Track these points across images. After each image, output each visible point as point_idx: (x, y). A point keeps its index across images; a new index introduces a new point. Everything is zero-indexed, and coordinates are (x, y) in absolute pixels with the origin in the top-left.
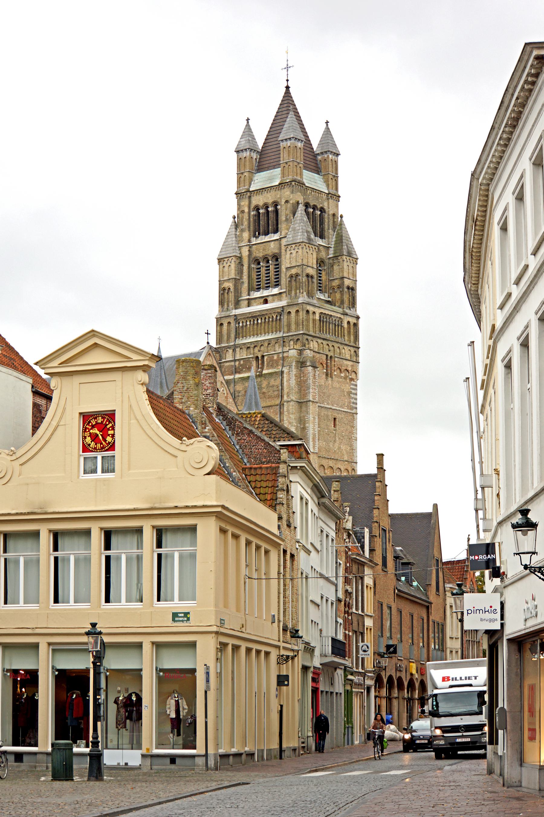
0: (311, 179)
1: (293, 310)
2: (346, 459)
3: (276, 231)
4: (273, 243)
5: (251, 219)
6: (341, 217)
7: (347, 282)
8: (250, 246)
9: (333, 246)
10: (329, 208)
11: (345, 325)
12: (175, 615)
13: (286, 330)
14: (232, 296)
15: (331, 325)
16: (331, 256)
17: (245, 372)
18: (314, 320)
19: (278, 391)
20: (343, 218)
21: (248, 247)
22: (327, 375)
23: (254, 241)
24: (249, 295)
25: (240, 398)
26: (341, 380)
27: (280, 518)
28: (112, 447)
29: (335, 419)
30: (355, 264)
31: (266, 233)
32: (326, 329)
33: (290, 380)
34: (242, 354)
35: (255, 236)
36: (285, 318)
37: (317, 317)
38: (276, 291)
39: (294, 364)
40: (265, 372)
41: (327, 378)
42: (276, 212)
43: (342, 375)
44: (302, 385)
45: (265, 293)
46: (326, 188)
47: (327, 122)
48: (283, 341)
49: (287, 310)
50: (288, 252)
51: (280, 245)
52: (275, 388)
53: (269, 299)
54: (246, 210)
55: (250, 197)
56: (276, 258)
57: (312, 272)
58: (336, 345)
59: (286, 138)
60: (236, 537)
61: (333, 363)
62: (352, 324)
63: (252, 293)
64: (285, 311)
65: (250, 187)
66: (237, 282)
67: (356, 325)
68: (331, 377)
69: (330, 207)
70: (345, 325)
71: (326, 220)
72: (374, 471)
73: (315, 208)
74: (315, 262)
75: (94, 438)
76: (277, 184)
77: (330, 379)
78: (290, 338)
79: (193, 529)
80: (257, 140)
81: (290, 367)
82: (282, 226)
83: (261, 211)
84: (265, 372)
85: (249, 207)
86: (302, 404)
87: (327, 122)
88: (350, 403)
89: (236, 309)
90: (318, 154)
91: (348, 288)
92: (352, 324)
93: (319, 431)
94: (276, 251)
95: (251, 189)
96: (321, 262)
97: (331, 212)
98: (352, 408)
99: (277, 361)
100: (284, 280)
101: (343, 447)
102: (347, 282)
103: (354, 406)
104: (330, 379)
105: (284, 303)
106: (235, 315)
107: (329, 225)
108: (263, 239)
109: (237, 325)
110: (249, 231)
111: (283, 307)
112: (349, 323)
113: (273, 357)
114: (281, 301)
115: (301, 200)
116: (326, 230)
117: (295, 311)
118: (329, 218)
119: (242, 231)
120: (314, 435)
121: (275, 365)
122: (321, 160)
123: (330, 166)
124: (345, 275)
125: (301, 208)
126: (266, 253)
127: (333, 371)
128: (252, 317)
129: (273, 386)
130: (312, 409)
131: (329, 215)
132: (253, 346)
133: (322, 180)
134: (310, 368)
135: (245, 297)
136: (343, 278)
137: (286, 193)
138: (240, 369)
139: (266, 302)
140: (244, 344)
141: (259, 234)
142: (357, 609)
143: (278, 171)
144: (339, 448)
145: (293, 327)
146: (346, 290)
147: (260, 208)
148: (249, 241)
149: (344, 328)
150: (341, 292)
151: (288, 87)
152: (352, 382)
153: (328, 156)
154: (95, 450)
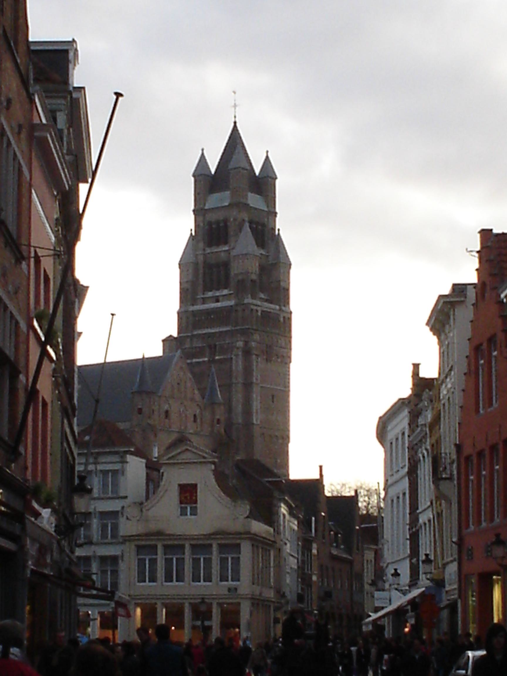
0: (254, 200)
3: (226, 243)
6: (279, 230)
8: (204, 255)
11: (282, 319)
12: (229, 590)
22: (267, 360)
23: (208, 250)
27: (274, 530)
28: (196, 502)
31: (218, 245)
33: (238, 365)
34: (198, 344)
37: (259, 314)
38: (225, 292)
39: (240, 353)
42: (226, 226)
43: (279, 360)
44: (248, 371)
45: (218, 294)
46: (266, 207)
53: (221, 299)
56: (226, 265)
57: (254, 277)
60: (257, 547)
63: (206, 292)
65: (205, 205)
67: (290, 319)
70: (282, 319)
72: (317, 477)
73: (257, 223)
74: (257, 269)
75: (186, 497)
76: (227, 204)
79: (238, 546)
81: (237, 355)
83: (214, 226)
84: (217, 358)
85: (203, 222)
86: (248, 385)
89: (193, 305)
91: (284, 289)
93: (261, 407)
96: (262, 268)
104: (269, 364)
105: (232, 303)
106: (193, 311)
108: (215, 249)
110: (204, 243)
111: (231, 306)
112: (284, 317)
114: (230, 300)
115: (246, 219)
120: (257, 410)
122: (264, 183)
125: (247, 224)
134: (254, 356)
137: (234, 213)
139: (218, 301)
142: (308, 570)
143: (228, 193)
148: (204, 250)
151: (235, 123)
154: (186, 503)
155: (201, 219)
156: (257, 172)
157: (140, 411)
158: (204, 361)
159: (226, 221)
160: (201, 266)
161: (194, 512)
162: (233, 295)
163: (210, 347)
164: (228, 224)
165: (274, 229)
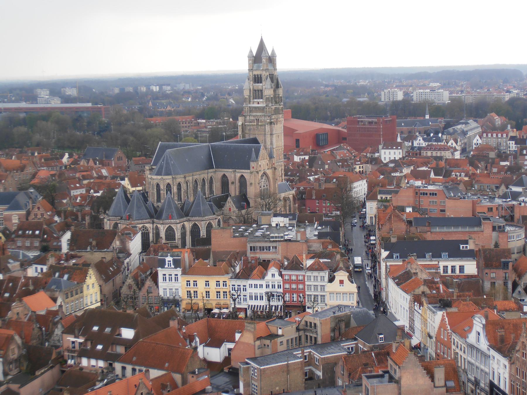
1: (268, 108)
3: (261, 83)
14: (248, 100)
23: (254, 85)
33: (268, 128)
34: (252, 118)
36: (265, 110)
38: (261, 100)
42: (261, 77)
44: (271, 130)
45: (258, 100)
48: (265, 116)
57: (272, 96)
66: (250, 96)
82: (264, 82)
86: (271, 134)
100: (264, 98)
105: (265, 105)
108: (257, 84)
130: (274, 136)
139: (258, 103)
155: (251, 73)
157: (253, 168)
160: (252, 90)
161: (343, 286)
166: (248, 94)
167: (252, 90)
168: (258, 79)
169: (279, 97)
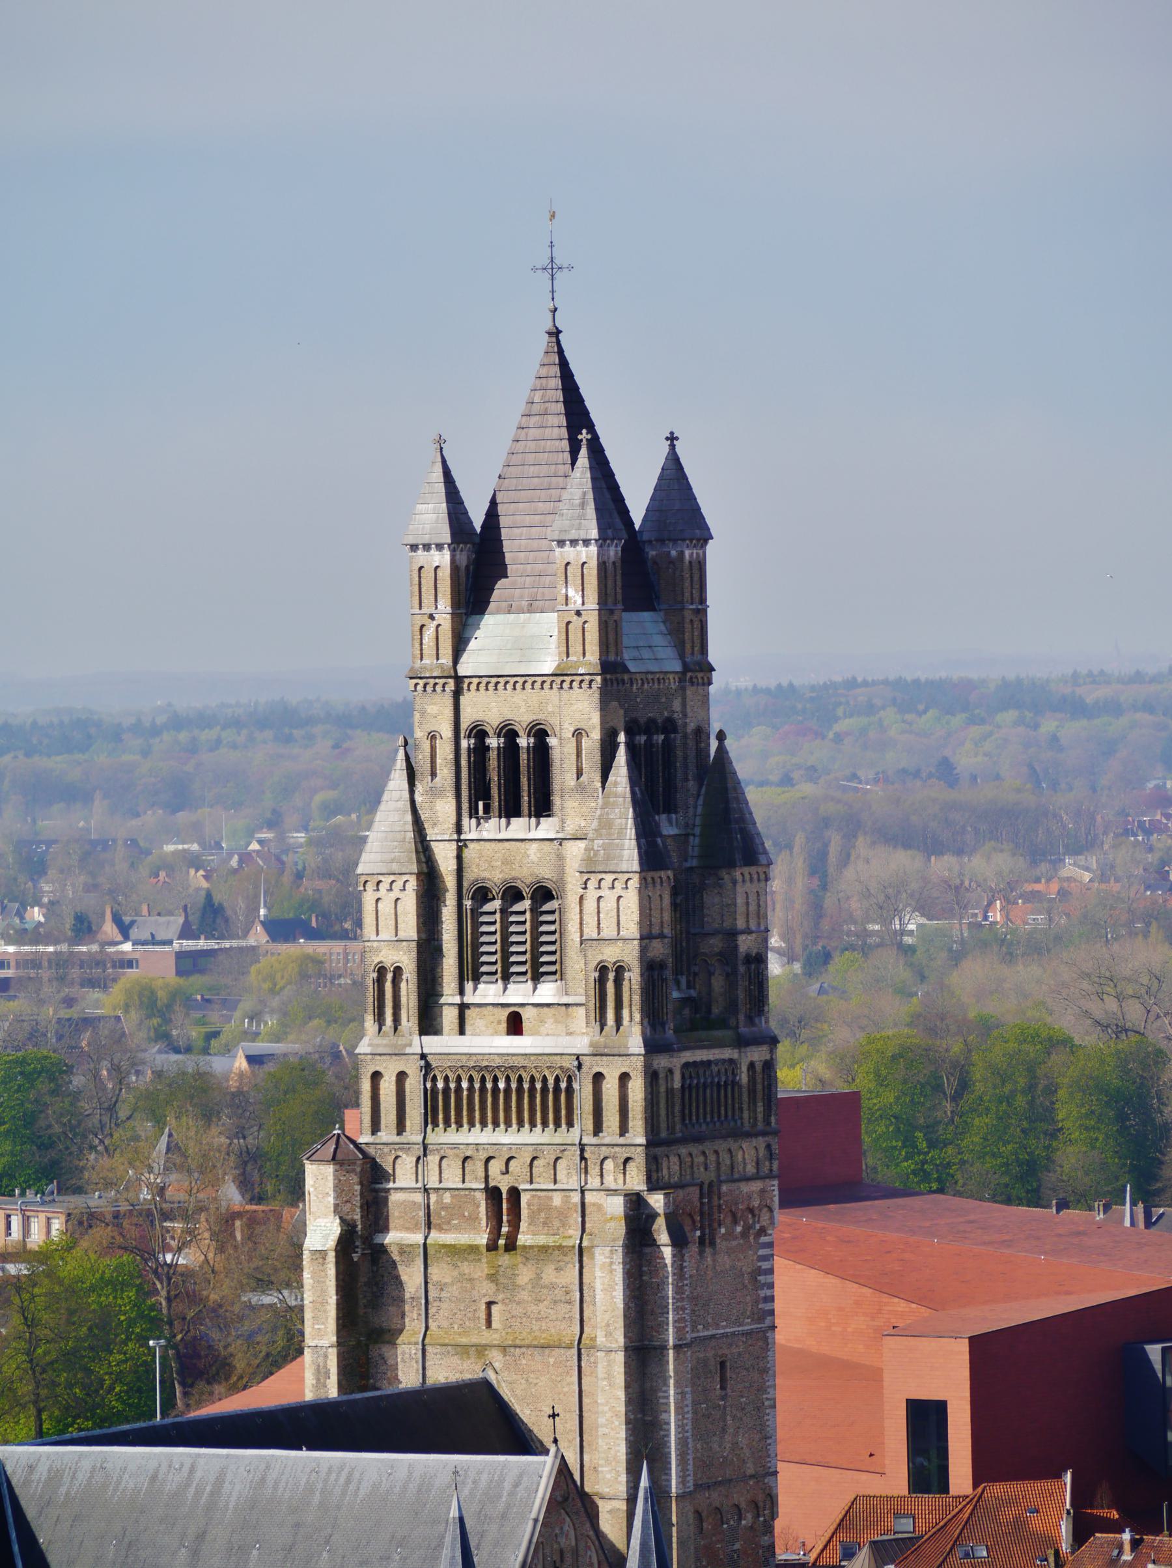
2: (750, 1471)
3: (543, 807)
4: (535, 845)
5: (464, 762)
6: (721, 736)
7: (745, 944)
9: (697, 831)
10: (685, 715)
11: (744, 1078)
13: (590, 1126)
15: (708, 1091)
16: (694, 863)
17: (458, 1228)
18: (670, 1092)
19: (569, 1302)
20: (726, 742)
21: (454, 846)
23: (471, 831)
24: (462, 992)
25: (444, 1306)
26: (734, 1243)
29: (722, 1364)
30: (763, 884)
31: (511, 810)
32: (698, 1107)
35: (473, 812)
38: (547, 991)
40: (523, 1239)
41: (701, 1253)
42: (541, 752)
45: (518, 993)
47: (672, 438)
49: (592, 1066)
50: (592, 894)
51: (560, 858)
52: (559, 1294)
53: (527, 1015)
54: (447, 731)
55: (457, 694)
57: (659, 949)
58: (722, 1146)
59: (573, 535)
61: (715, 1201)
62: (759, 1068)
64: (584, 1069)
68: (712, 1244)
69: (689, 710)
71: (679, 753)
73: (650, 727)
77: (708, 1250)
78: (605, 1151)
80: (468, 504)
87: (672, 438)
88: (757, 1302)
90: (650, 542)
92: (759, 1068)
94: (546, 874)
95: (462, 671)
97: (692, 726)
98: (761, 1319)
99: (562, 1214)
101: (742, 1440)
102: (745, 944)
103: (767, 1307)
104: (708, 1250)
107: (686, 766)
109: (429, 1085)
113: (551, 1198)
116: (679, 785)
117: (617, 1074)
118: (685, 745)
119: (434, 793)
121: (556, 1223)
123: (687, 583)
124: (741, 924)
126: (514, 874)
127: (716, 1225)
128: (481, 1069)
129: (552, 1287)
131: (685, 736)
132: (483, 1156)
133: (662, 627)
135: (449, 995)
136: (732, 934)
138: (440, 1217)
140: (455, 1146)
141: (487, 809)
144: (735, 1444)
145: (611, 1118)
146: (742, 969)
147: (491, 733)
148: (459, 829)
149: (740, 1087)
150: (728, 975)
151: (556, 333)
152: (763, 1239)
153: (682, 553)
156: (637, 515)
158: (473, 1249)
159: (540, 734)
162: (581, 1011)
163: (493, 1194)
164: (552, 741)
165: (701, 733)
166: (410, 928)
167: (450, 881)
168: (509, 775)
169: (729, 955)
